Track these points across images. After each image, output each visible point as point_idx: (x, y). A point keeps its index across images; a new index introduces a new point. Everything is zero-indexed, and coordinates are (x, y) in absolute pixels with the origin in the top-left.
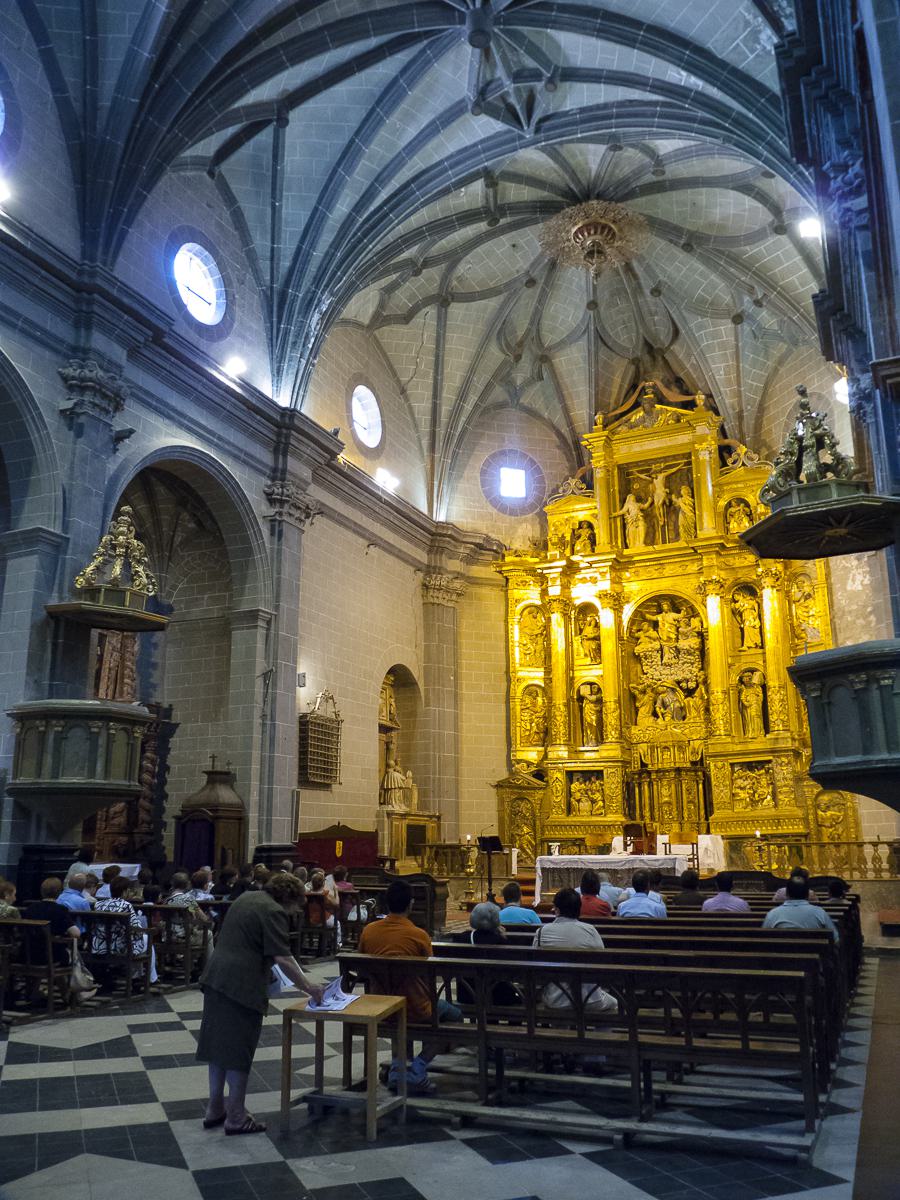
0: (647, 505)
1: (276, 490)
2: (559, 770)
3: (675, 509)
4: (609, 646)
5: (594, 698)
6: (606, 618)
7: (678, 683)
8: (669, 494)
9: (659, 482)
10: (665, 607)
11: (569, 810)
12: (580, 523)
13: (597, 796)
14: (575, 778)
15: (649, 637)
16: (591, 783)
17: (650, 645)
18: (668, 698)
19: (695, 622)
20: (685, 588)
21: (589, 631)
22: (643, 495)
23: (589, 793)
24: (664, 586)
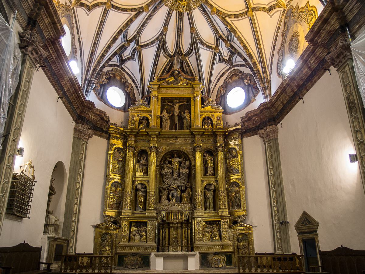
0: (170, 115)
1: (27, 35)
3: (182, 118)
4: (153, 169)
5: (143, 190)
6: (153, 156)
7: (178, 187)
8: (180, 112)
10: (176, 155)
11: (130, 240)
12: (143, 117)
13: (143, 233)
14: (133, 225)
15: (168, 167)
16: (140, 227)
18: (174, 192)
19: (188, 163)
20: (186, 149)
21: (143, 162)
22: (169, 111)
24: (177, 147)
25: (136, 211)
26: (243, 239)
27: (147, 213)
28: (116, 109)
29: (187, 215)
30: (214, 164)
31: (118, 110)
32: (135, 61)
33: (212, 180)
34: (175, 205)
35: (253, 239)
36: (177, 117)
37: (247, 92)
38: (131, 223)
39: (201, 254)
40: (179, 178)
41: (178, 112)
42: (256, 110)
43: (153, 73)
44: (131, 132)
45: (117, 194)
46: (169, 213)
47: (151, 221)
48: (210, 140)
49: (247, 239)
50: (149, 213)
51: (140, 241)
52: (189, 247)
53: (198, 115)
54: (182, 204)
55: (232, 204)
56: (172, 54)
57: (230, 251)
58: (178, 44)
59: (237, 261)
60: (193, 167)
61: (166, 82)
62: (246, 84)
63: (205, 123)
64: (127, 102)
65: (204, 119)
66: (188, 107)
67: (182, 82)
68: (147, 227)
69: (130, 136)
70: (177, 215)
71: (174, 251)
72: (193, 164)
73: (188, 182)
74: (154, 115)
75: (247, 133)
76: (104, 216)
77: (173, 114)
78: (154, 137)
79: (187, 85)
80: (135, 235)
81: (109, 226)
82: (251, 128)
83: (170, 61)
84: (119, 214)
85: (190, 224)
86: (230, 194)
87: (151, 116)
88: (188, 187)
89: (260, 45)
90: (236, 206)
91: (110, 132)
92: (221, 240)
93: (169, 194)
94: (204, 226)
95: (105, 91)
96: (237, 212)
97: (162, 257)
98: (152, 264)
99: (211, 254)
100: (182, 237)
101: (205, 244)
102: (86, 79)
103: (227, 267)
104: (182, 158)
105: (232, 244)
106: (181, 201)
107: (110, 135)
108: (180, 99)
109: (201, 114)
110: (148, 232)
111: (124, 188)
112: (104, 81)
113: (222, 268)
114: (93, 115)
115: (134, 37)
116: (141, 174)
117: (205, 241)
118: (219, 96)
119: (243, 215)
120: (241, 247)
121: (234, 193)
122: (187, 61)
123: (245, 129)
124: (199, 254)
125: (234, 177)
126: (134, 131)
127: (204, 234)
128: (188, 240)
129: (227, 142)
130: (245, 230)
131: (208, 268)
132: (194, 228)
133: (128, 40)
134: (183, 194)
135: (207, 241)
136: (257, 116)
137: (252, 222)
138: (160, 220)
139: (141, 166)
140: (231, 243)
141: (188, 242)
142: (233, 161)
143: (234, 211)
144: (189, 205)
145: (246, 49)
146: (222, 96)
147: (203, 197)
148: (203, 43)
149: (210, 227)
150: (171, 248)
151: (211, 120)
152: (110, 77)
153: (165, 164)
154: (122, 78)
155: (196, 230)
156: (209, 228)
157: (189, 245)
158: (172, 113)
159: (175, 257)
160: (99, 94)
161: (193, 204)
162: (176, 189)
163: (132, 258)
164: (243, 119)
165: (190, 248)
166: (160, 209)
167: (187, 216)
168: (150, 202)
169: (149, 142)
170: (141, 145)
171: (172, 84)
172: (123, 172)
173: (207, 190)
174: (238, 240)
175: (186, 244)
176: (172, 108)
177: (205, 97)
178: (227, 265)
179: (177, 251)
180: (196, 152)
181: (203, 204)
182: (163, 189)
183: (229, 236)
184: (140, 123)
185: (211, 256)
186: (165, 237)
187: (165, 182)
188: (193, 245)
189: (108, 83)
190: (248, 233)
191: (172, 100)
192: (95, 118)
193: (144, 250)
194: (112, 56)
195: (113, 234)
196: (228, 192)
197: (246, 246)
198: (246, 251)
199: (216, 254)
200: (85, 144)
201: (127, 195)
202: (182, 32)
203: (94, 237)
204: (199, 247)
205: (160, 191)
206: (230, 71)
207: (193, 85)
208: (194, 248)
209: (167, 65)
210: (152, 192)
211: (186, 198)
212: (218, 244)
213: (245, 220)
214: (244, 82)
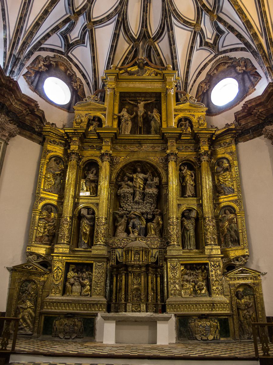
0: (133, 116)
2: (61, 261)
4: (104, 185)
5: (89, 216)
6: (105, 167)
7: (143, 214)
8: (145, 113)
9: (141, 105)
10: (139, 169)
12: (94, 117)
13: (86, 282)
14: (71, 269)
15: (128, 185)
16: (82, 272)
17: (128, 190)
18: (137, 222)
19: (156, 180)
20: (155, 159)
21: (91, 176)
23: (81, 279)
24: (141, 156)
25: (78, 248)
26: (245, 294)
27: (94, 249)
28: (56, 107)
29: (155, 255)
30: (195, 181)
31: (59, 108)
32: (86, 47)
33: (192, 203)
34: (137, 239)
35: (262, 294)
36: (141, 118)
37: (242, 81)
38: (68, 265)
39: (178, 316)
40: (144, 201)
41: (143, 111)
42: (260, 96)
43: (110, 61)
44: (74, 133)
45: (50, 222)
46: (128, 251)
47: (99, 262)
48: (189, 147)
49: (252, 293)
50: (97, 250)
51: (81, 293)
52: (158, 305)
53: (171, 114)
54: (148, 238)
55: (225, 239)
56: (136, 38)
57: (226, 312)
58: (144, 20)
59: (236, 329)
60: (164, 185)
61: (127, 72)
62: (240, 72)
63: (181, 126)
64: (74, 100)
65: (180, 120)
66: (157, 106)
67: (148, 72)
68: (92, 272)
69: (73, 140)
70: (139, 255)
71: (135, 312)
72: (164, 180)
73: (157, 208)
74: (109, 113)
75: (244, 135)
76: (28, 254)
77: (137, 116)
78: (108, 140)
79: (156, 75)
80: (74, 283)
81: (32, 268)
82: (250, 128)
83: (133, 47)
84: (52, 250)
85: (160, 268)
86: (221, 224)
87: (105, 115)
88: (156, 215)
89: (264, 6)
90: (232, 243)
91: (44, 133)
92: (210, 294)
93: (128, 224)
94: (182, 272)
95: (41, 81)
96: (234, 252)
97: (115, 321)
98: (97, 332)
99: (195, 318)
100: (148, 289)
101: (185, 301)
102: (11, 55)
103: (222, 339)
104: (148, 173)
105: (228, 302)
106: (146, 235)
107: (44, 139)
108: (144, 95)
109: (176, 113)
110: (93, 279)
111: (62, 214)
112: (41, 68)
113: (213, 341)
114: (18, 103)
115: (84, 8)
116: (88, 194)
117: (186, 296)
118: (200, 93)
119: (244, 256)
120: (243, 307)
121: (227, 223)
122: (156, 48)
123: (241, 130)
124: (176, 317)
125: (225, 200)
126: (78, 131)
127: (182, 285)
128: (157, 294)
129: (214, 150)
130: (248, 279)
131: (190, 342)
132: (165, 275)
133: (75, 11)
134: (149, 224)
135: (188, 296)
136: (260, 107)
137: (259, 267)
138: (114, 262)
139: (88, 183)
140: (226, 300)
141: (157, 297)
142: (223, 175)
143: (228, 249)
145: (242, 15)
146: (205, 93)
147: (180, 229)
148: (179, 17)
149: (192, 273)
150: (129, 306)
151: (190, 122)
152: (51, 64)
153: (123, 181)
154: (68, 69)
155: (170, 278)
156: (190, 276)
157: (159, 302)
158: (135, 113)
159: (136, 321)
160: (32, 83)
161: (164, 238)
162: (139, 218)
163: (67, 322)
164: (238, 115)
165: (160, 306)
166: (114, 246)
167: (155, 257)
168: (98, 233)
169: (101, 148)
170: (90, 154)
171: (136, 75)
172: (61, 191)
173: (186, 218)
174: (237, 295)
175: (154, 300)
176: (135, 109)
177: (181, 93)
178: (221, 336)
179: (140, 311)
180: (169, 161)
181: (180, 239)
183: (223, 289)
184: (89, 125)
185: (195, 321)
186: (121, 289)
187: (122, 208)
188: (165, 302)
189: (46, 71)
190: (254, 284)
191: (135, 97)
192: (21, 108)
193: (86, 309)
194: (52, 30)
195: (39, 282)
196: (218, 221)
197: (251, 305)
198: (251, 313)
199: (203, 318)
200: (3, 144)
201: (65, 222)
202: (150, 3)
203: (10, 285)
204: (174, 306)
205: (115, 220)
206: (215, 60)
207: (164, 74)
208: (167, 307)
209: (128, 54)
210: (102, 218)
211: (155, 230)
212: (206, 301)
213: (246, 263)
214: (236, 71)
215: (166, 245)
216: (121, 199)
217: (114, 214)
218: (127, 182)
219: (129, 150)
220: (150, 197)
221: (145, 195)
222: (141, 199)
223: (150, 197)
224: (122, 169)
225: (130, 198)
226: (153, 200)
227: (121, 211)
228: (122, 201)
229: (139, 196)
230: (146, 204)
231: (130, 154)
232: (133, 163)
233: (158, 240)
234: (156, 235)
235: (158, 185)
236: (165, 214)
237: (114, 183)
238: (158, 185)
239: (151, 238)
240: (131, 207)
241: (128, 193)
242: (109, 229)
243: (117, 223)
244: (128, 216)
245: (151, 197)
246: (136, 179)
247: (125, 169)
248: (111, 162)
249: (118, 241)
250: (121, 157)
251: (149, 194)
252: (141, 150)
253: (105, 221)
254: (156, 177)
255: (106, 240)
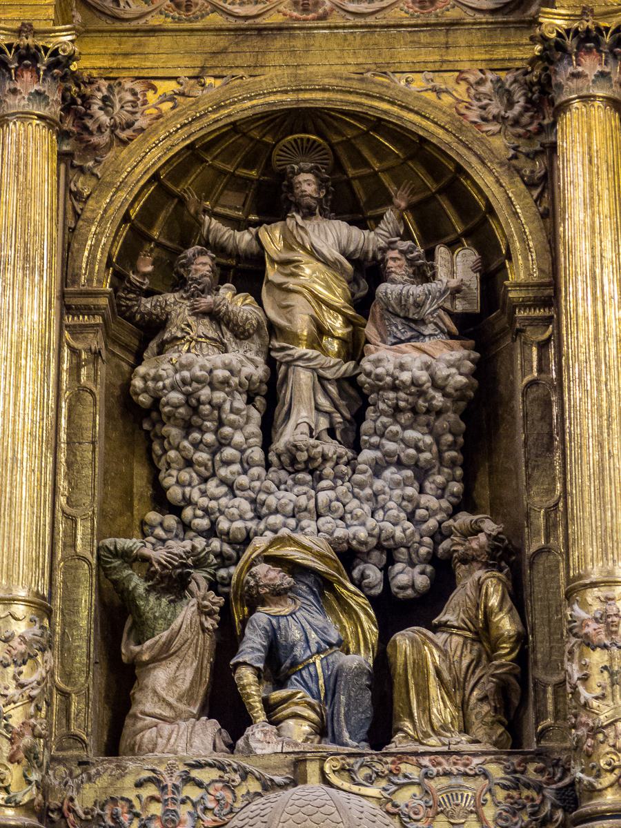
7: (349, 555)
10: (307, 185)
15: (214, 315)
17: (217, 358)
34: (312, 769)
40: (357, 447)
54: (402, 756)
60: (524, 305)
73: (465, 503)
88: (465, 560)
104: (390, 215)
134: (404, 641)
144: (496, 770)
153: (179, 283)
161: (539, 755)
162: (323, 587)
180: (565, 107)
182: (149, 576)
187: (176, 510)
211: (455, 688)
215: (559, 815)
216: (163, 438)
217: (106, 562)
218: (213, 289)
219: (216, 19)
220: (405, 417)
221: (365, 398)
222: (331, 432)
223: (405, 417)
224: (161, 188)
225: (236, 427)
226: (437, 441)
227: (163, 541)
228: (172, 454)
229: (318, 408)
230: (377, 474)
231: (223, 51)
232: (255, 134)
233: (485, 775)
234: (465, 730)
235: (476, 308)
236: (540, 551)
237: (103, 301)
238: (476, 308)
239: (425, 761)
240: (253, 501)
241: (225, 382)
242: (65, 695)
243: (139, 643)
244: (226, 582)
245: (414, 410)
246: (285, 263)
247: (187, 188)
248: (68, 125)
249: (151, 790)
250: (149, 82)
251: (395, 388)
252: (323, 17)
253: (36, 630)
254: (453, 246)
255: (43, 788)
